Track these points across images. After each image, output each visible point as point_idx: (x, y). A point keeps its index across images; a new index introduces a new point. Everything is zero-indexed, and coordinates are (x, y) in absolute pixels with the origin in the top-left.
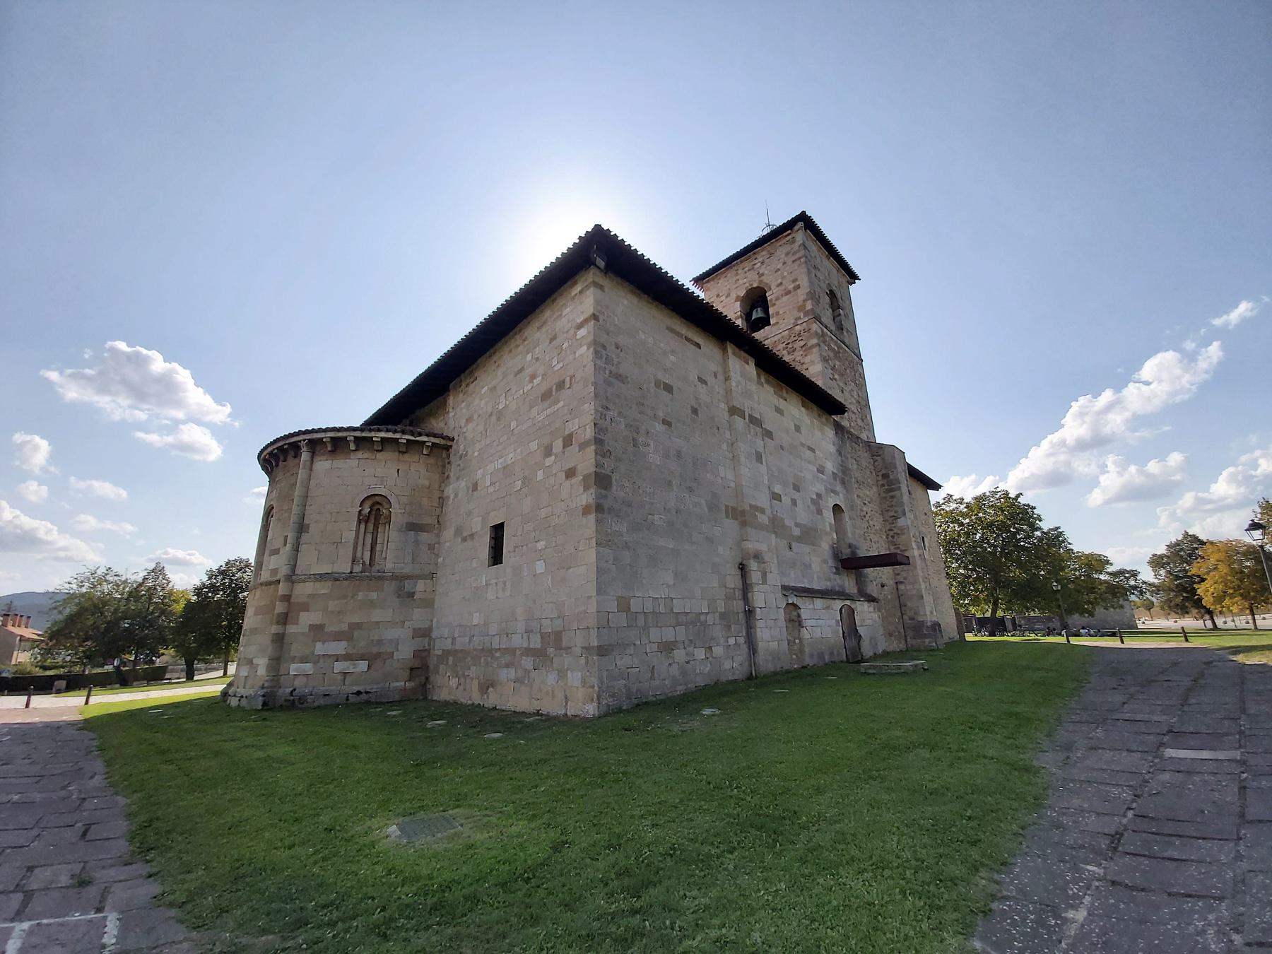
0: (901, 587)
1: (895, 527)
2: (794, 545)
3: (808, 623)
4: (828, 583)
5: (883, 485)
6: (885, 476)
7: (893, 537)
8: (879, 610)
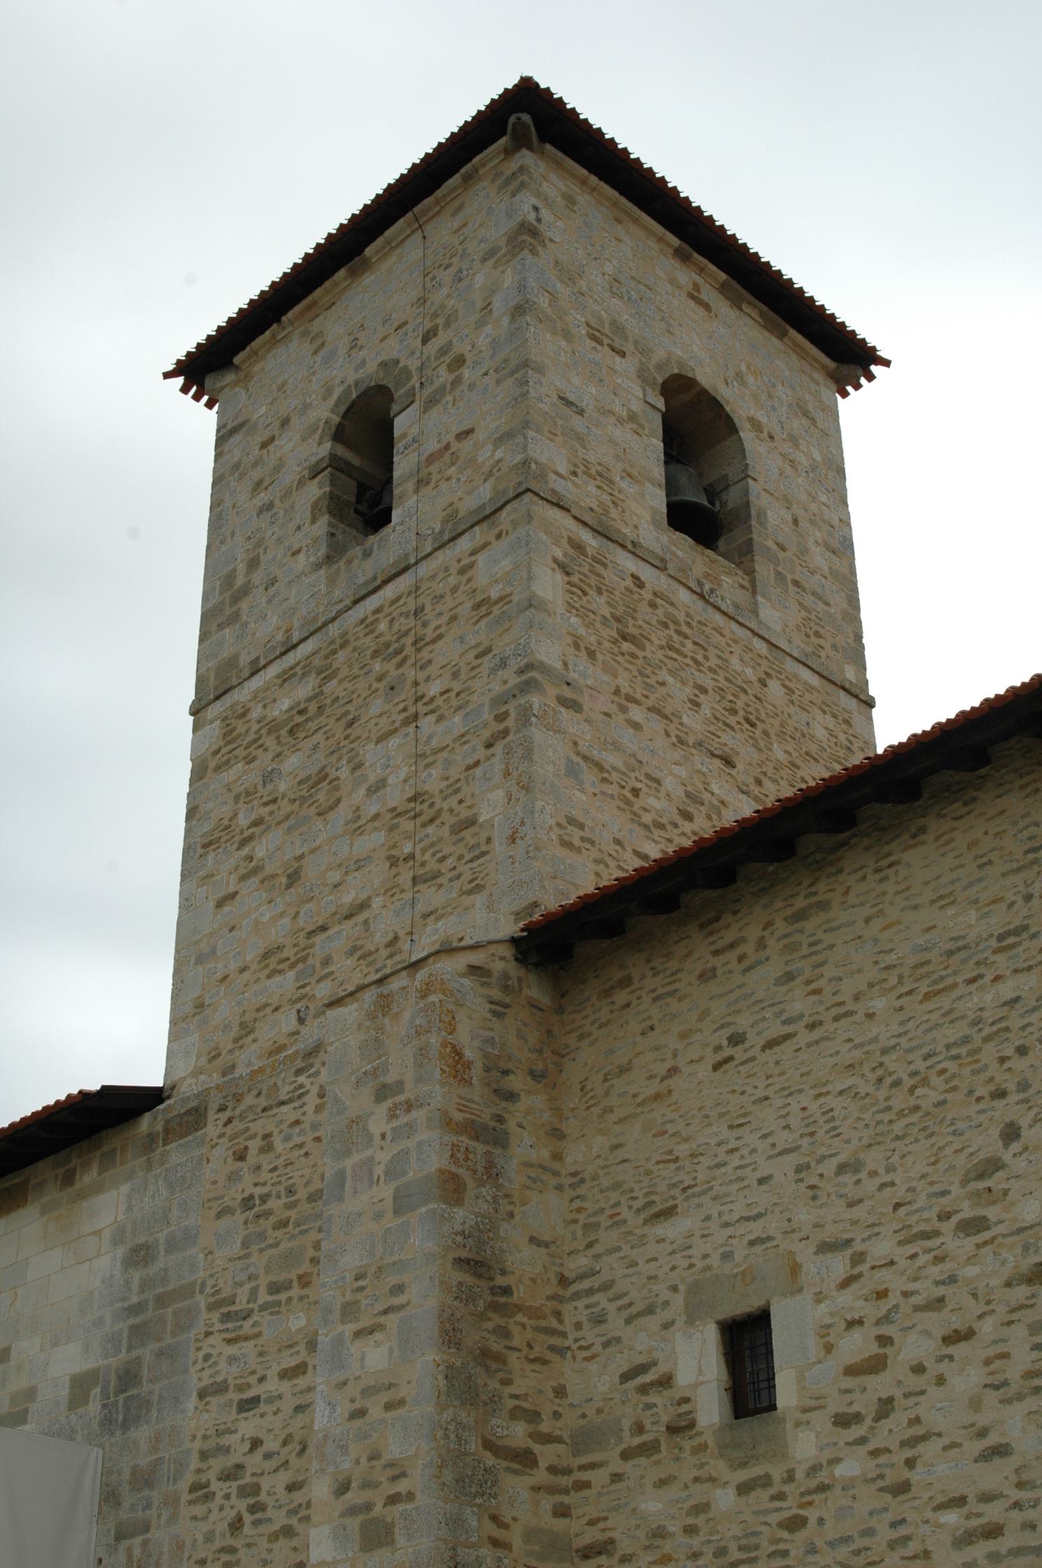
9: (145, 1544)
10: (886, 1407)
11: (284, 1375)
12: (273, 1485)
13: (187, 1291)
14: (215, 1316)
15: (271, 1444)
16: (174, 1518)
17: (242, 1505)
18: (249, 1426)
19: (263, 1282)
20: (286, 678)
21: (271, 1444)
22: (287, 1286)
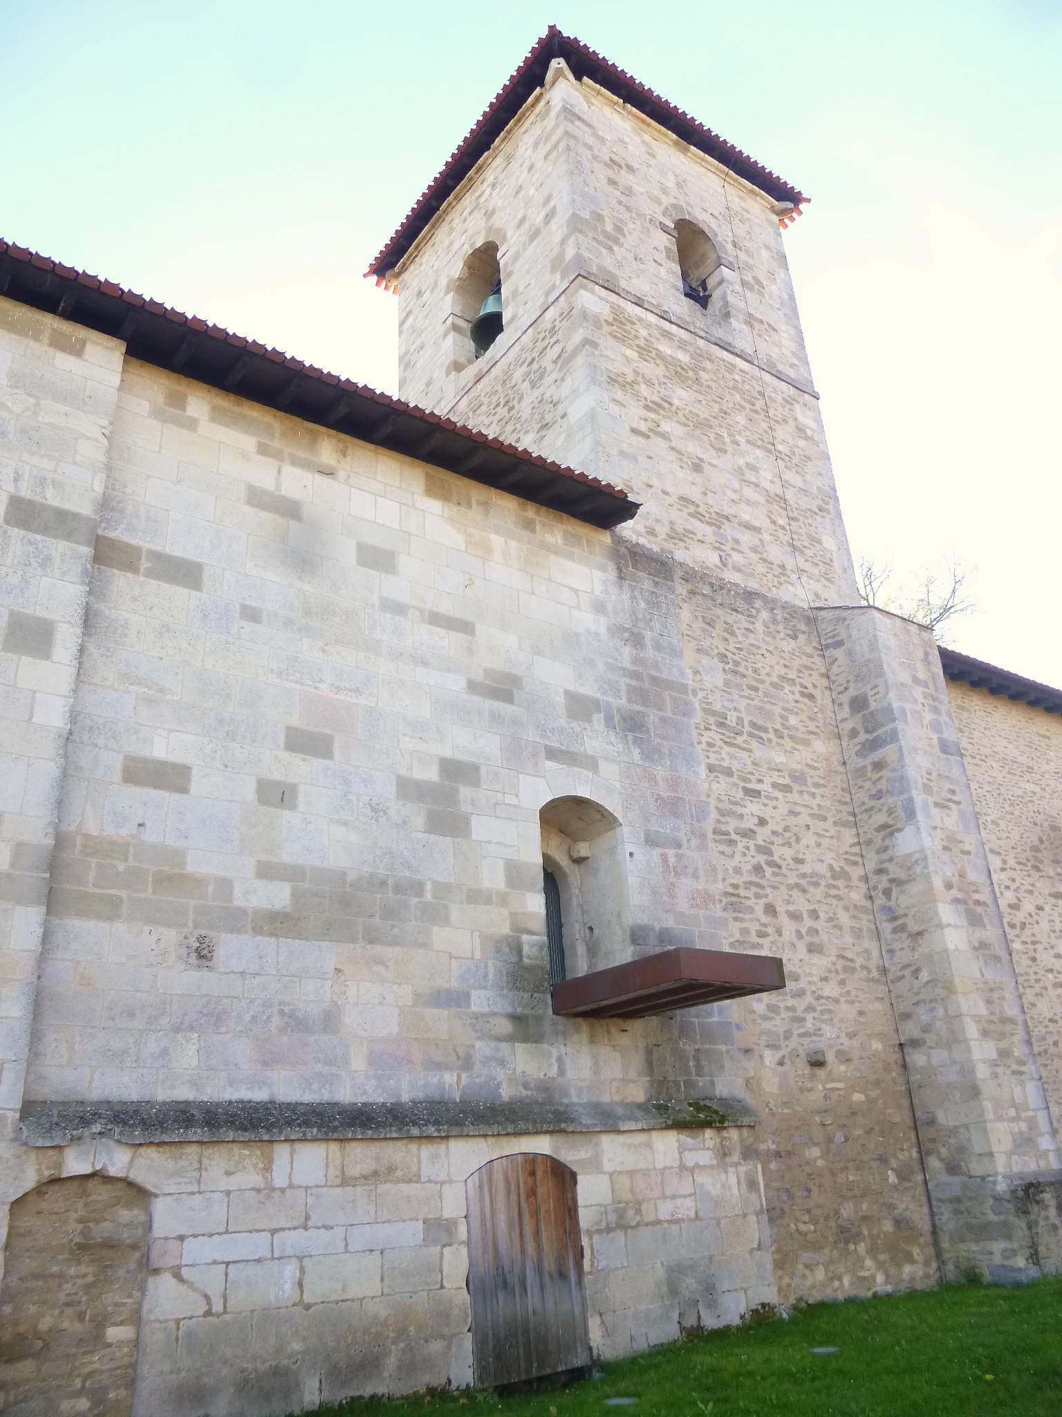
0: (918, 1059)
1: (891, 860)
2: (232, 949)
3: (195, 1250)
4: (449, 1078)
5: (854, 733)
6: (859, 704)
7: (887, 893)
8: (749, 1153)
9: (679, 857)
10: (1023, 925)
11: (775, 786)
12: (782, 853)
13: (683, 689)
14: (711, 720)
15: (772, 825)
16: (702, 847)
17: (762, 859)
18: (753, 808)
19: (747, 719)
20: (666, 334)
21: (772, 825)
22: (766, 731)
